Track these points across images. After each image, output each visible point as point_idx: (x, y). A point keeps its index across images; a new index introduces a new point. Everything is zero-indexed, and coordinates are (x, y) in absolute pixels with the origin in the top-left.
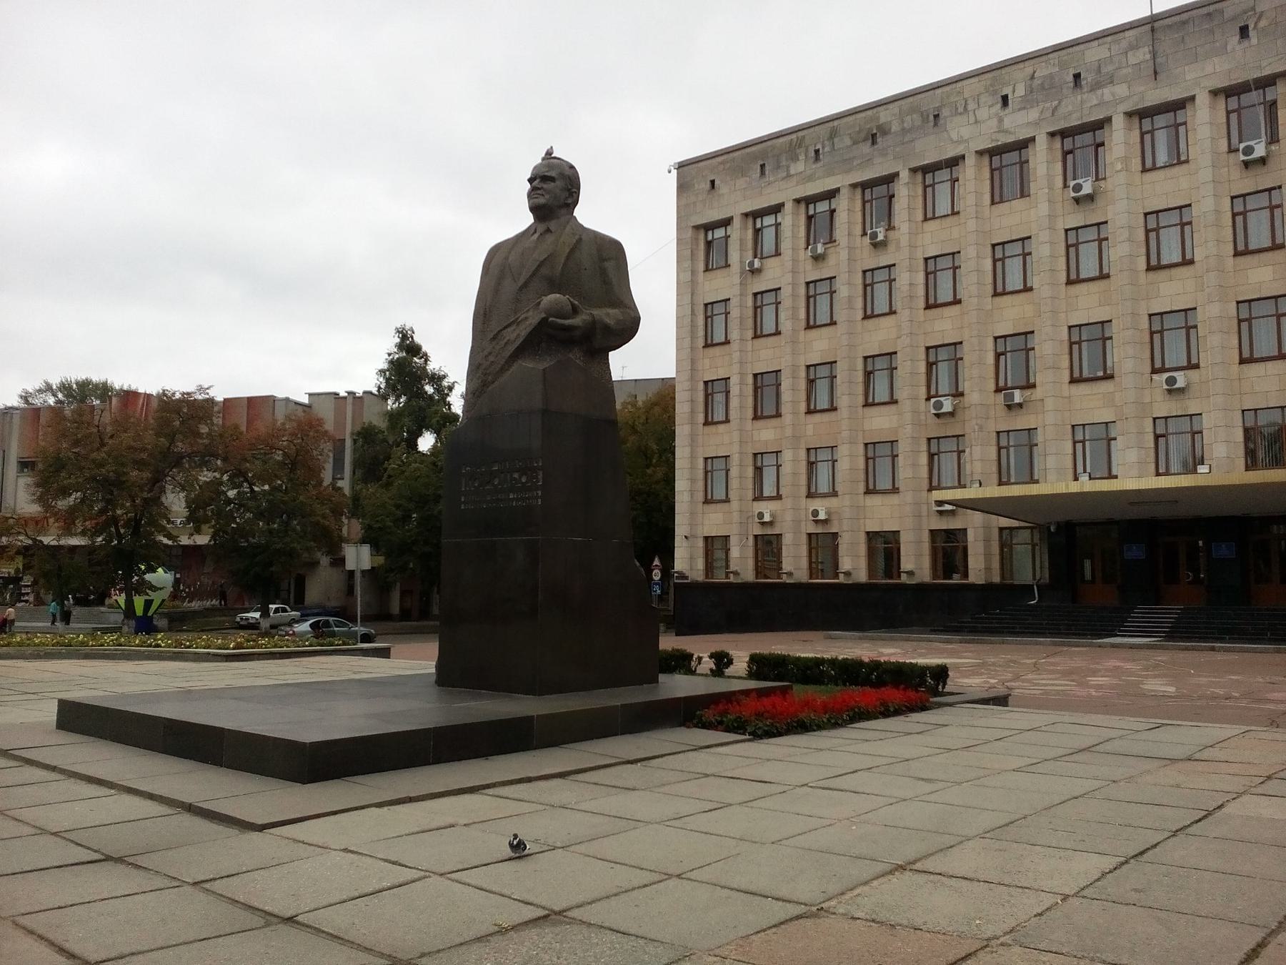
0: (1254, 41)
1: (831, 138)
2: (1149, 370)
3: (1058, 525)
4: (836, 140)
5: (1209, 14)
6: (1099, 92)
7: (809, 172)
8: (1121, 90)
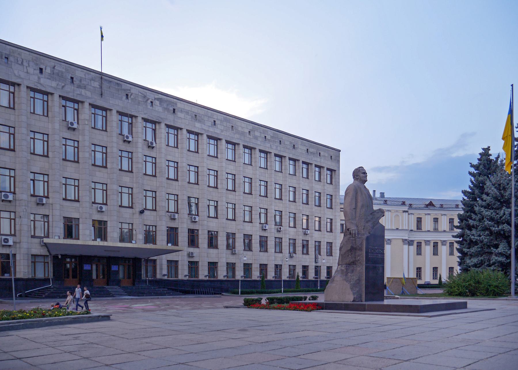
0: (130, 101)
6: (81, 90)
8: (89, 94)
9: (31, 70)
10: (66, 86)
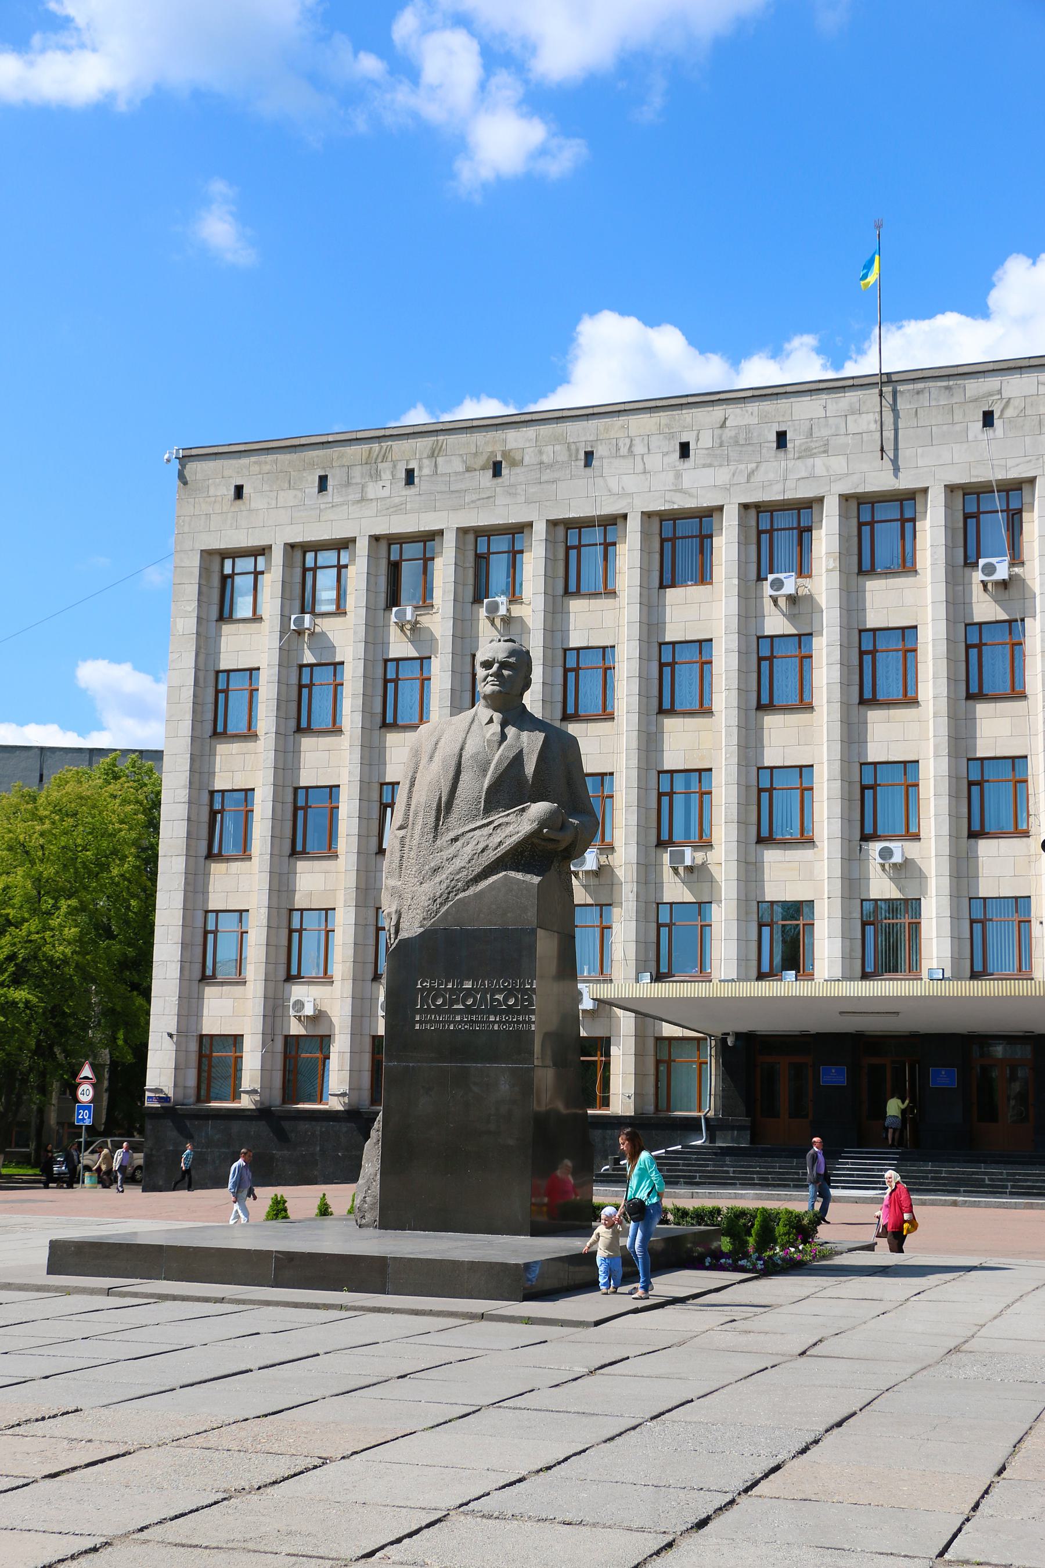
1: (433, 455)
2: (858, 837)
3: (738, 1035)
4: (439, 459)
5: (948, 388)
6: (810, 461)
7: (397, 500)
8: (838, 464)
9: (654, 462)
10: (763, 467)
